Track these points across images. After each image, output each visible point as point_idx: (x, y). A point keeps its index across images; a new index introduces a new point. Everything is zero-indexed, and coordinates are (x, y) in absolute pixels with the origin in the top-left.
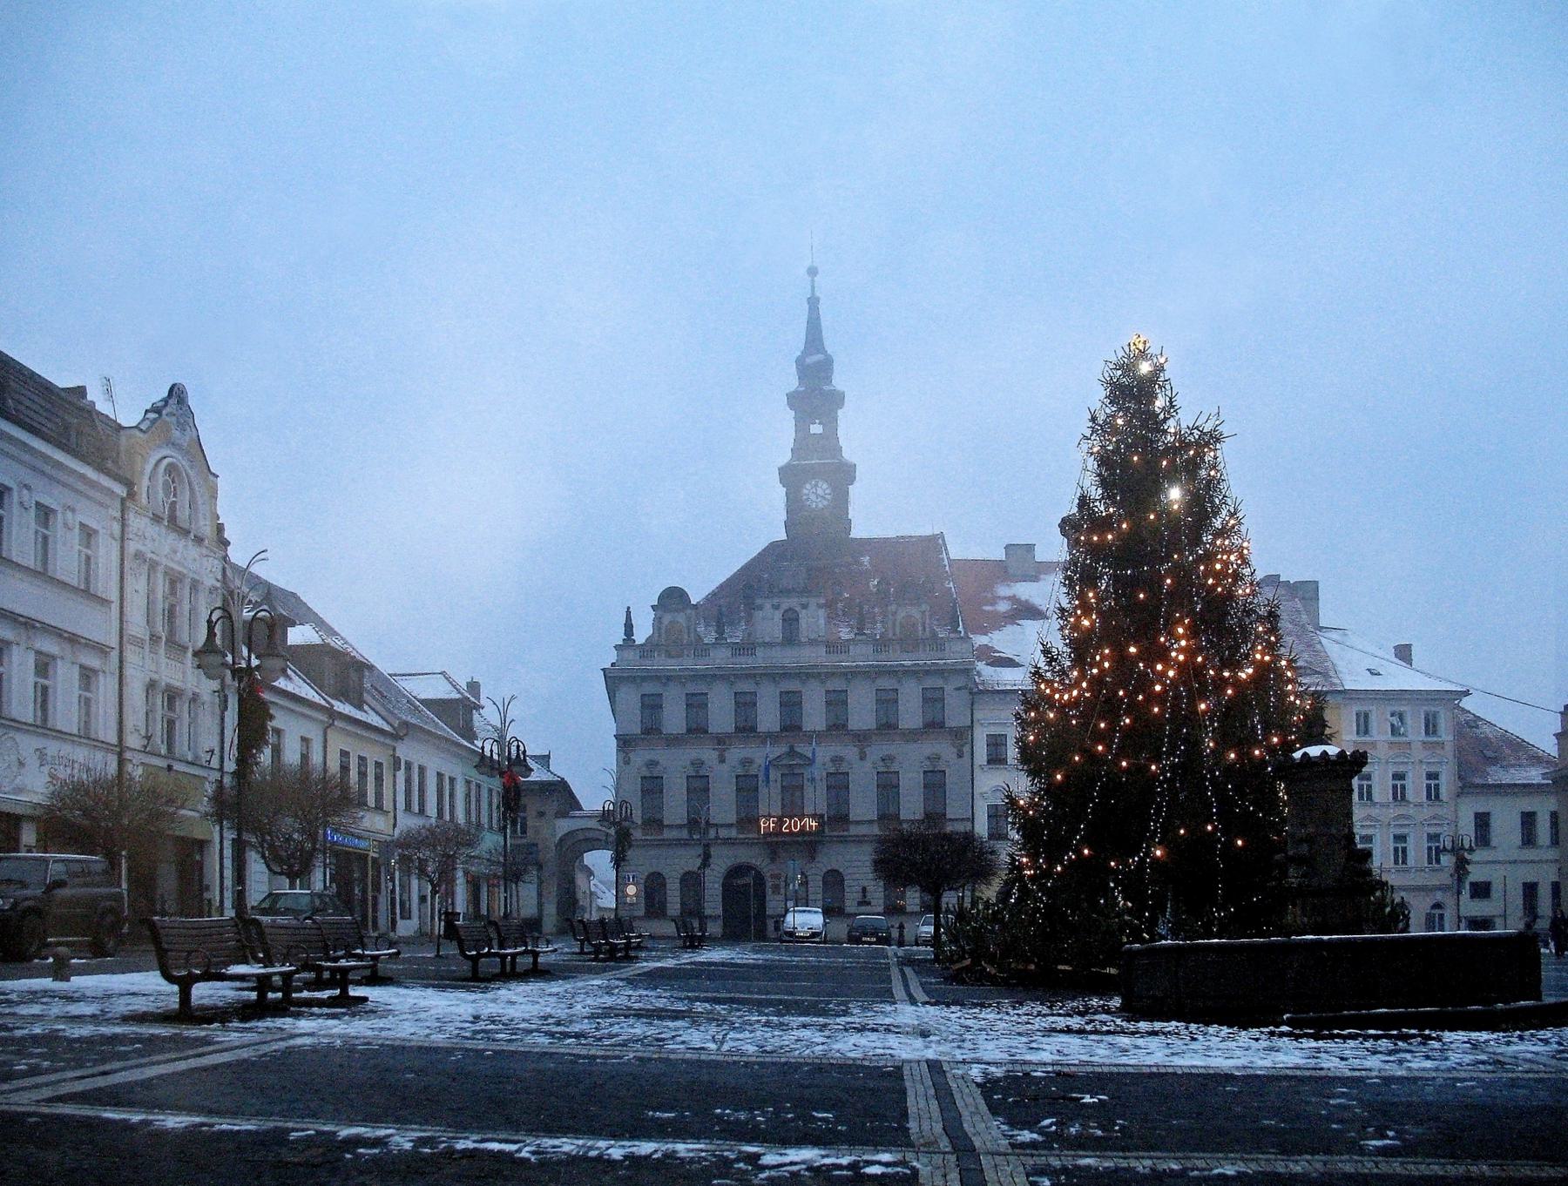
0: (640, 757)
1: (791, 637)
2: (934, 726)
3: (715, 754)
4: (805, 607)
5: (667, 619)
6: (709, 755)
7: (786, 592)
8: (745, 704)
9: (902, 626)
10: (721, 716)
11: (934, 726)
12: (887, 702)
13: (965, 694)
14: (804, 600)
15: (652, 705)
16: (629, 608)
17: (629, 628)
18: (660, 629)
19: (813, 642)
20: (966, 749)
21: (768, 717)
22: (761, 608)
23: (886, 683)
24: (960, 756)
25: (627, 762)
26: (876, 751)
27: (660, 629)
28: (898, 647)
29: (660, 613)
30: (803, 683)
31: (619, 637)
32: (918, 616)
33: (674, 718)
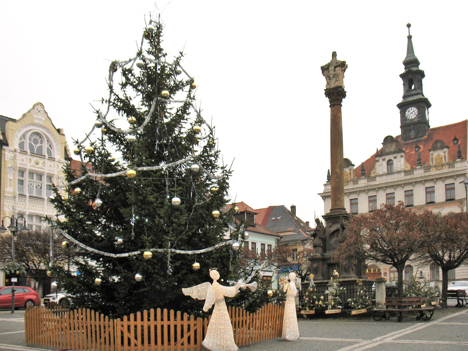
4: (395, 158)
7: (388, 154)
9: (436, 159)
13: (463, 185)
14: (395, 155)
19: (399, 172)
22: (378, 161)
30: (395, 189)
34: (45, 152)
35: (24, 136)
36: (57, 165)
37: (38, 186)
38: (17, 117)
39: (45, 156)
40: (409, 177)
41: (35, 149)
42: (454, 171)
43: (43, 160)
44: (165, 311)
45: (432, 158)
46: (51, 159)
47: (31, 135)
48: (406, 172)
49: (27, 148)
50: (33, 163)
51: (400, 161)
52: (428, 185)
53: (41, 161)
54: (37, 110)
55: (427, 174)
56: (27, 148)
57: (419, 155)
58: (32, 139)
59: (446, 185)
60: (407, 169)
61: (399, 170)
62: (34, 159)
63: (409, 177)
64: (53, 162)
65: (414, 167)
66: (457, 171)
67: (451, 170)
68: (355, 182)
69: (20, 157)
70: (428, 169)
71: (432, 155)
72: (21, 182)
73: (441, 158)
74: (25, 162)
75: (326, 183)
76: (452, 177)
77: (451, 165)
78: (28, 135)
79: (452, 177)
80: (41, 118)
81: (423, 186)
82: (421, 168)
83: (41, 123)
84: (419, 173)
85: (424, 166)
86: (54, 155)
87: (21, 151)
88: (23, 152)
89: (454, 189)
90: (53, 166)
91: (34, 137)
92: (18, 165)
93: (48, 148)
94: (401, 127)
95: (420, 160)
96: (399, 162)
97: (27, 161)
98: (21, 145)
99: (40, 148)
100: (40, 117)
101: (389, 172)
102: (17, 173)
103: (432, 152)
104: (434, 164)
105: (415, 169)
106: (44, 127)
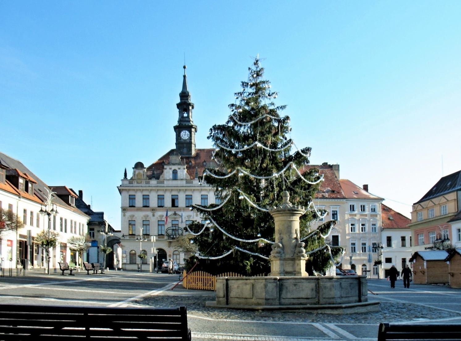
0: (128, 214)
1: (175, 178)
4: (179, 169)
5: (137, 172)
6: (150, 213)
7: (174, 164)
8: (161, 198)
10: (153, 202)
14: (179, 167)
15: (132, 198)
18: (135, 175)
19: (182, 179)
21: (168, 203)
22: (166, 169)
25: (124, 215)
27: (135, 175)
29: (135, 169)
33: (139, 202)
44: (203, 272)
51: (183, 172)
60: (188, 179)
61: (182, 178)
75: (123, 179)
94: (176, 144)
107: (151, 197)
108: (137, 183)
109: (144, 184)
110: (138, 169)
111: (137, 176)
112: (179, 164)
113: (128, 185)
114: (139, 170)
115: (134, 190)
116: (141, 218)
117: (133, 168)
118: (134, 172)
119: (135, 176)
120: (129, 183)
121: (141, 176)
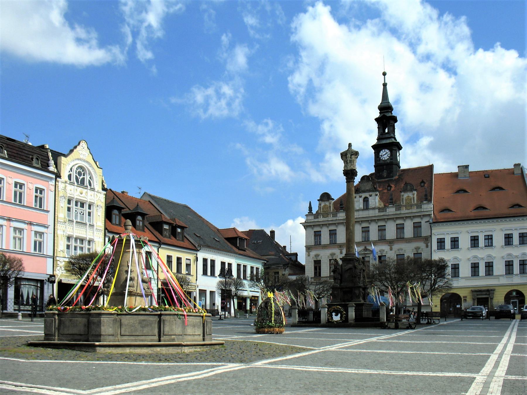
0: (313, 253)
2: (417, 236)
3: (339, 251)
4: (371, 196)
5: (323, 204)
7: (364, 192)
9: (406, 200)
11: (417, 236)
12: (400, 228)
14: (371, 193)
15: (317, 235)
16: (310, 202)
17: (310, 208)
19: (374, 209)
20: (429, 244)
23: (399, 222)
24: (427, 247)
25: (309, 255)
26: (396, 247)
27: (320, 208)
28: (404, 208)
29: (320, 202)
31: (307, 211)
32: (412, 196)
33: (325, 239)
34: (86, 183)
35: (71, 169)
36: (96, 195)
37: (82, 212)
38: (66, 153)
39: (87, 187)
40: (382, 214)
41: (80, 180)
42: (422, 212)
43: (86, 190)
45: (403, 199)
46: (93, 189)
47: (77, 169)
48: (380, 209)
49: (73, 179)
50: (78, 193)
51: (375, 199)
52: (399, 222)
53: (84, 191)
54: (82, 146)
55: (398, 212)
56: (73, 179)
57: (391, 195)
58: (77, 171)
59: (413, 223)
60: (381, 207)
61: (373, 206)
62: (80, 189)
63: (382, 214)
64: (93, 192)
65: (387, 204)
66: (424, 212)
67: (419, 210)
68: (335, 215)
69: (69, 187)
70: (399, 208)
71: (403, 196)
72: (69, 209)
73: (411, 199)
74: (72, 191)
76: (419, 216)
77: (419, 206)
78: (75, 169)
79: (419, 216)
80: (85, 154)
81: (394, 222)
82: (393, 207)
83: (84, 158)
84: (391, 210)
85: (395, 205)
86: (94, 186)
87: (70, 182)
88: (72, 184)
89: (420, 226)
90: (93, 196)
91: (78, 170)
92: (68, 195)
93: (89, 180)
95: (392, 199)
96: (374, 199)
97: (74, 191)
98: (70, 177)
99: (83, 180)
100: (84, 153)
101: (365, 207)
102: (66, 201)
103: (403, 193)
104: (404, 204)
105: (388, 207)
106: (87, 162)
107: (322, 233)
108: (323, 217)
109: (330, 218)
110: (324, 201)
111: (323, 209)
112: (369, 191)
113: (313, 221)
114: (326, 202)
115: (319, 225)
116: (327, 257)
117: (318, 200)
118: (320, 204)
119: (320, 210)
120: (315, 218)
121: (327, 208)
